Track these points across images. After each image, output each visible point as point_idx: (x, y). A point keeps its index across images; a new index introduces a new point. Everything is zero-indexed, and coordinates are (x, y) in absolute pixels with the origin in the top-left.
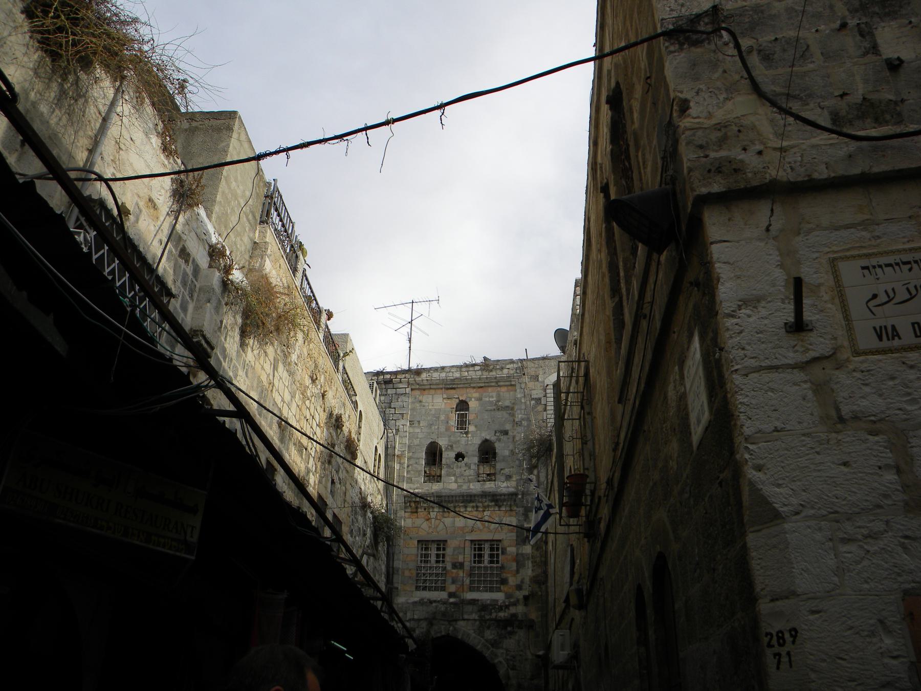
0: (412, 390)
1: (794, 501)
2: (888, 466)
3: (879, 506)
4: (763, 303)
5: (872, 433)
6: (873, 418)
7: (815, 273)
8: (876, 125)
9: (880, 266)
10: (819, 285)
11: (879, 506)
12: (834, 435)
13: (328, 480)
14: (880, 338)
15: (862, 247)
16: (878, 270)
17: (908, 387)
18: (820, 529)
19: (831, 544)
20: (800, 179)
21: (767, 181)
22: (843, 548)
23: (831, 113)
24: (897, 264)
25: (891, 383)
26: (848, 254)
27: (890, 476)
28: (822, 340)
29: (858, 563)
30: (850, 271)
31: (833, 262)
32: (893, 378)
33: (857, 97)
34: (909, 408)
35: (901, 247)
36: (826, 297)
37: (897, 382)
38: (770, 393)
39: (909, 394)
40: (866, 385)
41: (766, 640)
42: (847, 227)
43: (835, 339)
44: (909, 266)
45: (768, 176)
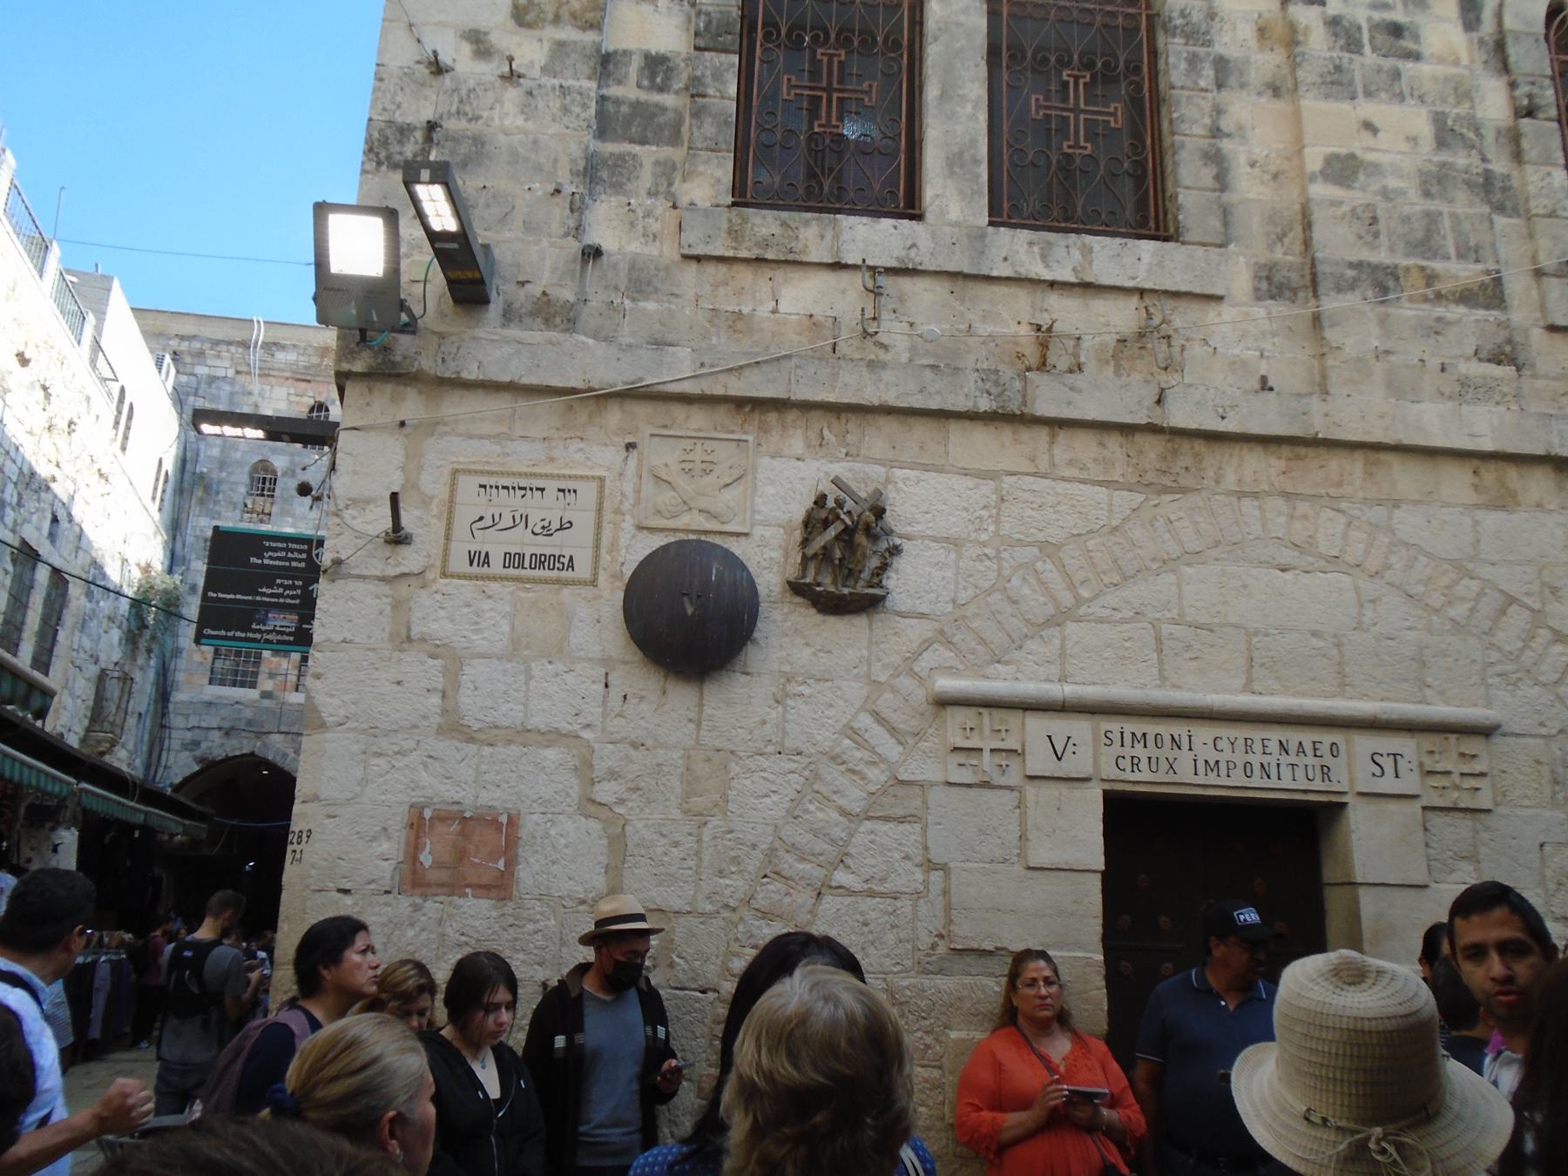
0: (238, 372)
1: (342, 712)
2: (435, 690)
3: (416, 726)
4: (371, 507)
5: (433, 657)
6: (438, 642)
7: (434, 483)
8: (543, 327)
9: (497, 487)
10: (432, 498)
11: (416, 726)
12: (397, 653)
13: (45, 518)
14: (471, 564)
15: (488, 463)
16: (494, 490)
17: (478, 616)
18: (358, 741)
19: (363, 757)
20: (447, 375)
21: (414, 370)
22: (375, 761)
23: (505, 301)
24: (514, 488)
25: (465, 610)
26: (472, 467)
27: (436, 700)
28: (416, 555)
29: (381, 776)
30: (468, 485)
31: (455, 472)
32: (468, 606)
33: (535, 290)
34: (474, 637)
35: (525, 470)
36: (435, 511)
37: (470, 610)
38: (350, 603)
39: (477, 623)
40: (442, 608)
41: (290, 837)
42: (481, 437)
43: (429, 557)
44: (523, 492)
45: (416, 364)
